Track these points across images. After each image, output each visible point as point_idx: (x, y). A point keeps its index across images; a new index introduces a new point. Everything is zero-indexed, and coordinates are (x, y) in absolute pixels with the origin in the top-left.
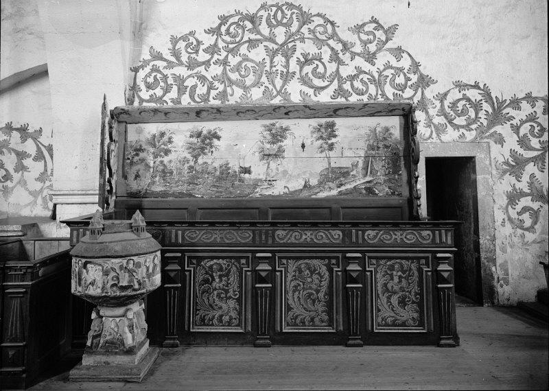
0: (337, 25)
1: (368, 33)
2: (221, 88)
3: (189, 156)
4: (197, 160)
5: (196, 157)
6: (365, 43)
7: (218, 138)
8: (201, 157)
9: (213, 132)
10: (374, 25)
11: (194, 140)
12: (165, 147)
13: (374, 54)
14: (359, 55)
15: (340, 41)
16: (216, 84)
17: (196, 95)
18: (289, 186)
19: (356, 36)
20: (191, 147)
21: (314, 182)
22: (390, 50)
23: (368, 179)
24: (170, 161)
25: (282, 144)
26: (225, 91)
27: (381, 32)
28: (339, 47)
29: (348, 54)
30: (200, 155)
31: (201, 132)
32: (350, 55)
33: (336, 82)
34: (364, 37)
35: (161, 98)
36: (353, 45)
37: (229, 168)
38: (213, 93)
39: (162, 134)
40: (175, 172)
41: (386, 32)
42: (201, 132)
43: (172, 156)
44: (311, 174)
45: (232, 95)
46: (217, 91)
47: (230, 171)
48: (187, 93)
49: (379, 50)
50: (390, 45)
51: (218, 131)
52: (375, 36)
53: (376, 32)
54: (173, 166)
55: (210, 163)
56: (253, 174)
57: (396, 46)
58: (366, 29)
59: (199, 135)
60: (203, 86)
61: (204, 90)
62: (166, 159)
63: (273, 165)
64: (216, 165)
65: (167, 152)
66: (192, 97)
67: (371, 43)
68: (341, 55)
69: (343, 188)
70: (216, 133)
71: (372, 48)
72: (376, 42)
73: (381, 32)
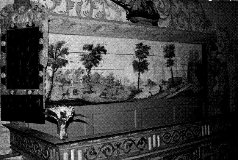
2: (101, 8)
3: (83, 67)
4: (90, 71)
5: (89, 67)
7: (105, 51)
8: (92, 68)
9: (101, 46)
11: (87, 52)
12: (63, 58)
16: (98, 5)
17: (82, 11)
18: (151, 91)
20: (85, 58)
21: (165, 88)
23: (190, 84)
24: (68, 73)
25: (146, 59)
26: (104, 11)
30: (91, 66)
31: (92, 46)
33: (170, 16)
35: (51, 10)
37: (113, 78)
38: (95, 12)
39: (60, 44)
40: (72, 82)
42: (92, 46)
43: (69, 67)
44: (164, 82)
45: (108, 16)
46: (97, 11)
47: (114, 80)
48: (74, 8)
51: (105, 46)
54: (71, 76)
55: (100, 74)
56: (130, 81)
59: (90, 47)
60: (87, 4)
61: (89, 7)
62: (64, 69)
63: (142, 76)
64: (105, 75)
65: (64, 63)
66: (78, 12)
69: (179, 91)
70: (103, 47)
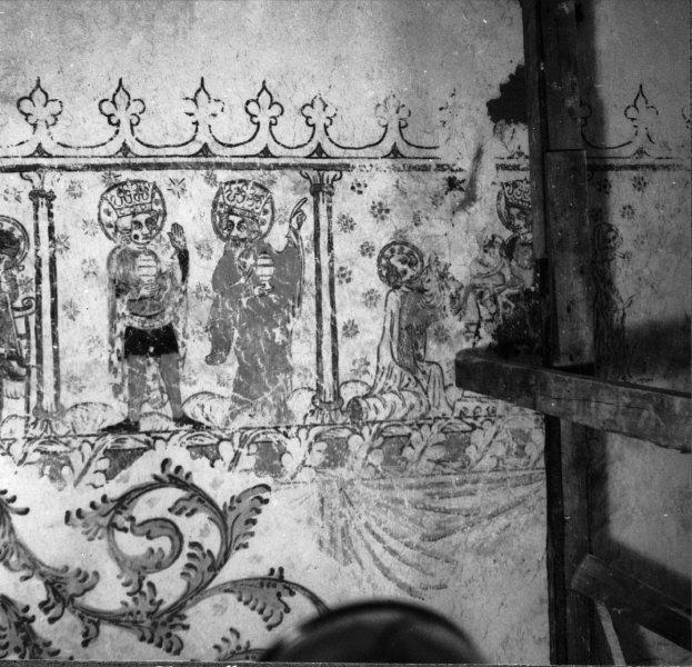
0: (18, 505)
1: (149, 529)
6: (138, 574)
10: (172, 494)
13: (177, 611)
14: (115, 619)
15: (33, 566)
19: (100, 545)
22: (234, 587)
27: (202, 518)
28: (31, 593)
29: (69, 619)
32: (78, 622)
34: (133, 545)
36: (87, 580)
41: (220, 516)
49: (195, 592)
50: (236, 567)
52: (177, 534)
53: (181, 521)
57: (262, 571)
58: (142, 510)
67: (159, 567)
68: (41, 625)
71: (169, 585)
72: (183, 560)
73: (196, 527)
